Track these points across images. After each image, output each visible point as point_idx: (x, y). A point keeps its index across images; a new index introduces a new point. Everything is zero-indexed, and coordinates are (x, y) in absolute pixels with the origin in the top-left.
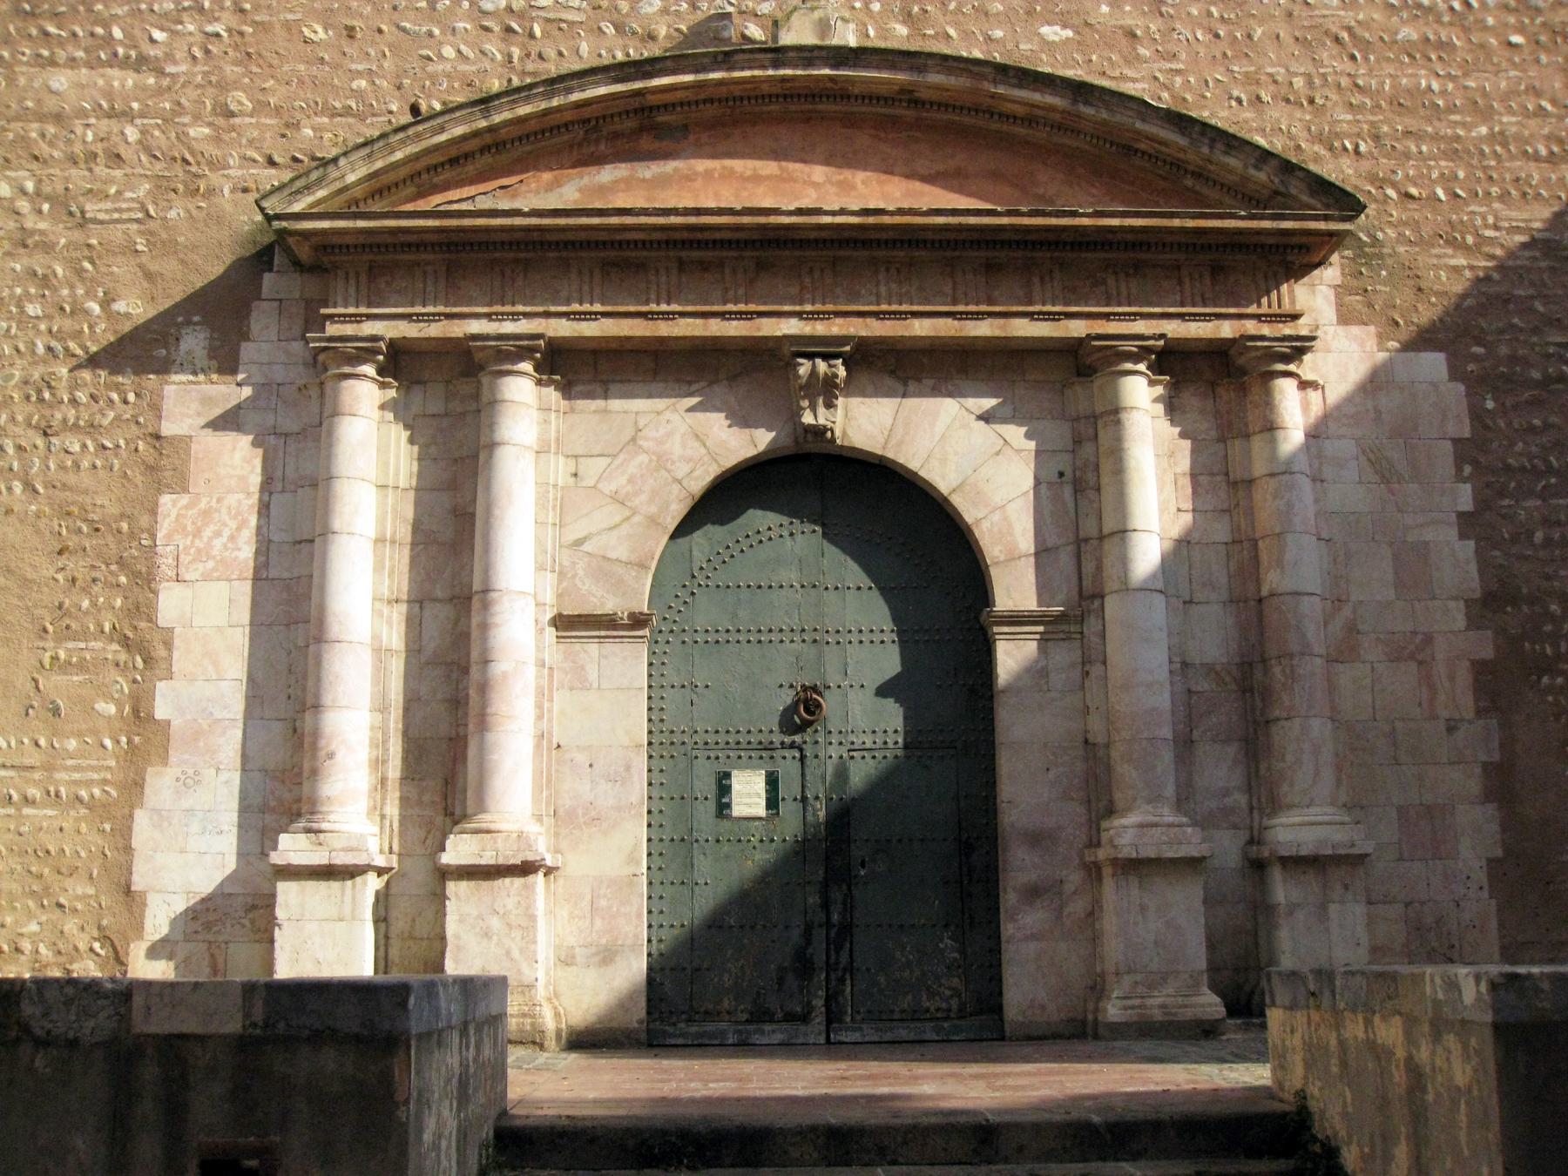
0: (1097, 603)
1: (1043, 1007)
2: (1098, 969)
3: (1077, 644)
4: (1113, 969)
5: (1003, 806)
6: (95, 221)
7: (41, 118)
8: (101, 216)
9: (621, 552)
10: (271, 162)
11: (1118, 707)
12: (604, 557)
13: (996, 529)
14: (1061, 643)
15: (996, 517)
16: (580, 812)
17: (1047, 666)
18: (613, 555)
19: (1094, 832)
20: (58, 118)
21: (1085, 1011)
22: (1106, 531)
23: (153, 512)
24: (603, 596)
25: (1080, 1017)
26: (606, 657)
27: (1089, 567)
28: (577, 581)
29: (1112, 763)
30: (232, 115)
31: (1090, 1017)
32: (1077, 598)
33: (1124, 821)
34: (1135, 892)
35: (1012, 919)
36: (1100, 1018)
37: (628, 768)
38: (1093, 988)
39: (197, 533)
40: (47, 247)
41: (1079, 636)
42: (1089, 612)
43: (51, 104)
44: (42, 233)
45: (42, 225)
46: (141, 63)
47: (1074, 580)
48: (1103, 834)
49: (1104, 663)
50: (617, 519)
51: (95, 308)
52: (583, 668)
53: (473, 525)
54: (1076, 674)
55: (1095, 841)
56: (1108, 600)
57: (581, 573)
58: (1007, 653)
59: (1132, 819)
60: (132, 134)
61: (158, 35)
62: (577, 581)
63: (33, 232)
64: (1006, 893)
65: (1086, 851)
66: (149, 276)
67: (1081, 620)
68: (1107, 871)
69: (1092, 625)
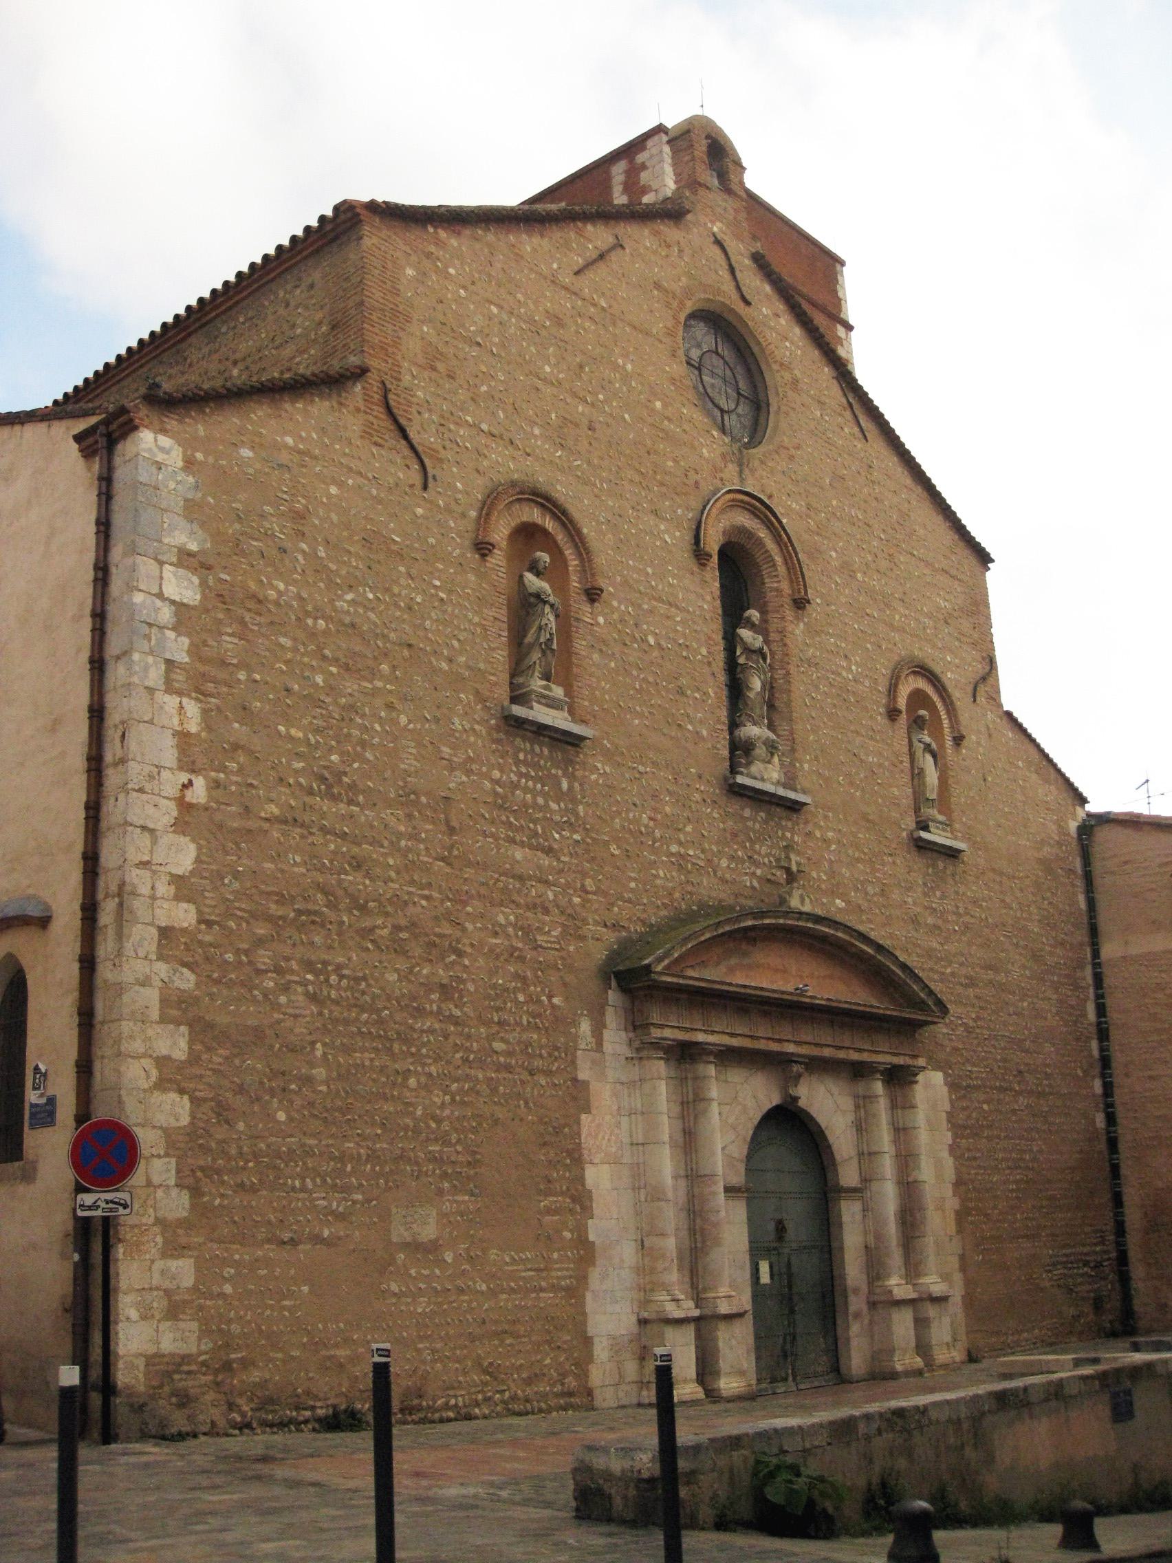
6: (541, 946)
7: (513, 877)
8: (544, 944)
10: (605, 925)
20: (520, 878)
23: (579, 1124)
30: (588, 892)
39: (596, 1137)
40: (522, 959)
43: (518, 870)
44: (520, 950)
45: (520, 945)
46: (549, 851)
51: (544, 998)
60: (551, 895)
61: (557, 836)
63: (517, 949)
66: (565, 985)
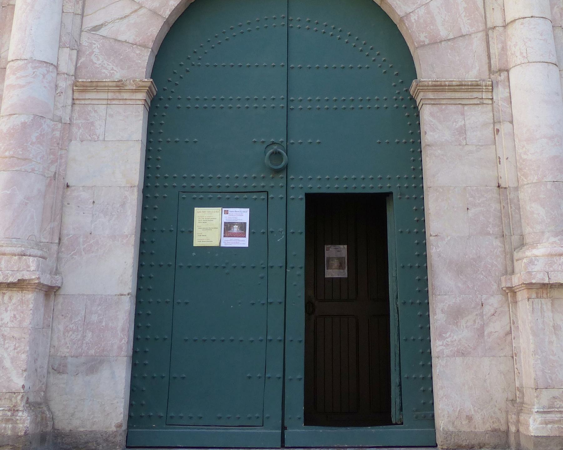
0: (504, 75)
1: (470, 418)
2: (517, 384)
3: (490, 107)
4: (532, 383)
5: (431, 240)
9: (128, 35)
11: (524, 157)
12: (116, 40)
13: (422, 21)
14: (476, 107)
15: (422, 11)
16: (81, 240)
17: (465, 125)
18: (122, 38)
19: (509, 263)
21: (507, 423)
22: (508, 20)
24: (112, 69)
25: (503, 428)
26: (111, 116)
27: (495, 49)
28: (93, 57)
29: (521, 203)
31: (513, 429)
32: (487, 73)
33: (536, 252)
34: (548, 314)
35: (441, 336)
36: (522, 429)
37: (123, 205)
38: (513, 401)
41: (490, 102)
42: (497, 83)
47: (485, 59)
48: (516, 263)
49: (512, 122)
50: (128, 11)
52: (92, 123)
53: (13, 13)
54: (489, 132)
55: (509, 269)
56: (512, 73)
57: (97, 51)
58: (432, 114)
59: (540, 251)
62: (93, 57)
64: (435, 314)
65: (503, 278)
67: (492, 87)
68: (522, 295)
69: (500, 93)
